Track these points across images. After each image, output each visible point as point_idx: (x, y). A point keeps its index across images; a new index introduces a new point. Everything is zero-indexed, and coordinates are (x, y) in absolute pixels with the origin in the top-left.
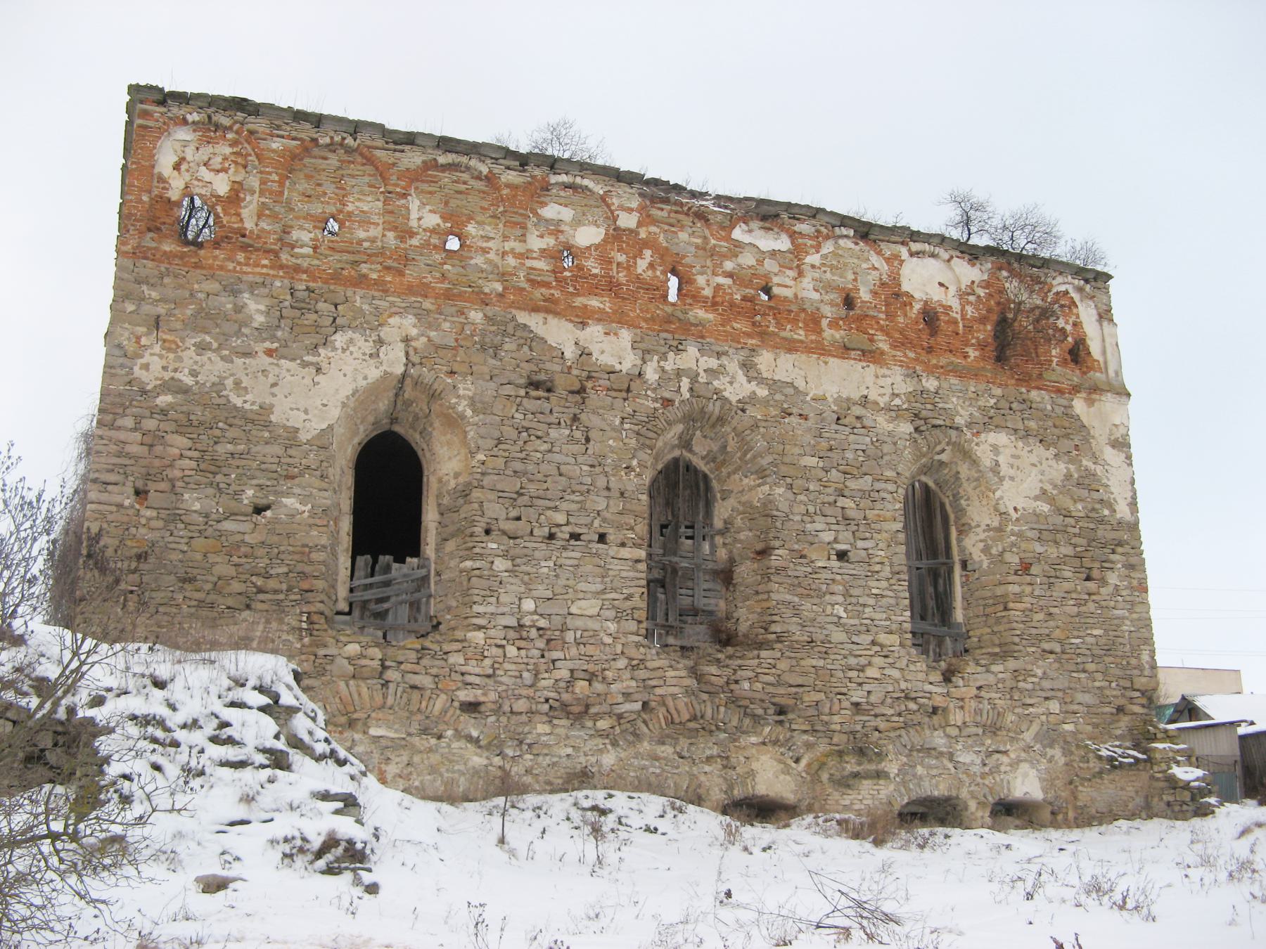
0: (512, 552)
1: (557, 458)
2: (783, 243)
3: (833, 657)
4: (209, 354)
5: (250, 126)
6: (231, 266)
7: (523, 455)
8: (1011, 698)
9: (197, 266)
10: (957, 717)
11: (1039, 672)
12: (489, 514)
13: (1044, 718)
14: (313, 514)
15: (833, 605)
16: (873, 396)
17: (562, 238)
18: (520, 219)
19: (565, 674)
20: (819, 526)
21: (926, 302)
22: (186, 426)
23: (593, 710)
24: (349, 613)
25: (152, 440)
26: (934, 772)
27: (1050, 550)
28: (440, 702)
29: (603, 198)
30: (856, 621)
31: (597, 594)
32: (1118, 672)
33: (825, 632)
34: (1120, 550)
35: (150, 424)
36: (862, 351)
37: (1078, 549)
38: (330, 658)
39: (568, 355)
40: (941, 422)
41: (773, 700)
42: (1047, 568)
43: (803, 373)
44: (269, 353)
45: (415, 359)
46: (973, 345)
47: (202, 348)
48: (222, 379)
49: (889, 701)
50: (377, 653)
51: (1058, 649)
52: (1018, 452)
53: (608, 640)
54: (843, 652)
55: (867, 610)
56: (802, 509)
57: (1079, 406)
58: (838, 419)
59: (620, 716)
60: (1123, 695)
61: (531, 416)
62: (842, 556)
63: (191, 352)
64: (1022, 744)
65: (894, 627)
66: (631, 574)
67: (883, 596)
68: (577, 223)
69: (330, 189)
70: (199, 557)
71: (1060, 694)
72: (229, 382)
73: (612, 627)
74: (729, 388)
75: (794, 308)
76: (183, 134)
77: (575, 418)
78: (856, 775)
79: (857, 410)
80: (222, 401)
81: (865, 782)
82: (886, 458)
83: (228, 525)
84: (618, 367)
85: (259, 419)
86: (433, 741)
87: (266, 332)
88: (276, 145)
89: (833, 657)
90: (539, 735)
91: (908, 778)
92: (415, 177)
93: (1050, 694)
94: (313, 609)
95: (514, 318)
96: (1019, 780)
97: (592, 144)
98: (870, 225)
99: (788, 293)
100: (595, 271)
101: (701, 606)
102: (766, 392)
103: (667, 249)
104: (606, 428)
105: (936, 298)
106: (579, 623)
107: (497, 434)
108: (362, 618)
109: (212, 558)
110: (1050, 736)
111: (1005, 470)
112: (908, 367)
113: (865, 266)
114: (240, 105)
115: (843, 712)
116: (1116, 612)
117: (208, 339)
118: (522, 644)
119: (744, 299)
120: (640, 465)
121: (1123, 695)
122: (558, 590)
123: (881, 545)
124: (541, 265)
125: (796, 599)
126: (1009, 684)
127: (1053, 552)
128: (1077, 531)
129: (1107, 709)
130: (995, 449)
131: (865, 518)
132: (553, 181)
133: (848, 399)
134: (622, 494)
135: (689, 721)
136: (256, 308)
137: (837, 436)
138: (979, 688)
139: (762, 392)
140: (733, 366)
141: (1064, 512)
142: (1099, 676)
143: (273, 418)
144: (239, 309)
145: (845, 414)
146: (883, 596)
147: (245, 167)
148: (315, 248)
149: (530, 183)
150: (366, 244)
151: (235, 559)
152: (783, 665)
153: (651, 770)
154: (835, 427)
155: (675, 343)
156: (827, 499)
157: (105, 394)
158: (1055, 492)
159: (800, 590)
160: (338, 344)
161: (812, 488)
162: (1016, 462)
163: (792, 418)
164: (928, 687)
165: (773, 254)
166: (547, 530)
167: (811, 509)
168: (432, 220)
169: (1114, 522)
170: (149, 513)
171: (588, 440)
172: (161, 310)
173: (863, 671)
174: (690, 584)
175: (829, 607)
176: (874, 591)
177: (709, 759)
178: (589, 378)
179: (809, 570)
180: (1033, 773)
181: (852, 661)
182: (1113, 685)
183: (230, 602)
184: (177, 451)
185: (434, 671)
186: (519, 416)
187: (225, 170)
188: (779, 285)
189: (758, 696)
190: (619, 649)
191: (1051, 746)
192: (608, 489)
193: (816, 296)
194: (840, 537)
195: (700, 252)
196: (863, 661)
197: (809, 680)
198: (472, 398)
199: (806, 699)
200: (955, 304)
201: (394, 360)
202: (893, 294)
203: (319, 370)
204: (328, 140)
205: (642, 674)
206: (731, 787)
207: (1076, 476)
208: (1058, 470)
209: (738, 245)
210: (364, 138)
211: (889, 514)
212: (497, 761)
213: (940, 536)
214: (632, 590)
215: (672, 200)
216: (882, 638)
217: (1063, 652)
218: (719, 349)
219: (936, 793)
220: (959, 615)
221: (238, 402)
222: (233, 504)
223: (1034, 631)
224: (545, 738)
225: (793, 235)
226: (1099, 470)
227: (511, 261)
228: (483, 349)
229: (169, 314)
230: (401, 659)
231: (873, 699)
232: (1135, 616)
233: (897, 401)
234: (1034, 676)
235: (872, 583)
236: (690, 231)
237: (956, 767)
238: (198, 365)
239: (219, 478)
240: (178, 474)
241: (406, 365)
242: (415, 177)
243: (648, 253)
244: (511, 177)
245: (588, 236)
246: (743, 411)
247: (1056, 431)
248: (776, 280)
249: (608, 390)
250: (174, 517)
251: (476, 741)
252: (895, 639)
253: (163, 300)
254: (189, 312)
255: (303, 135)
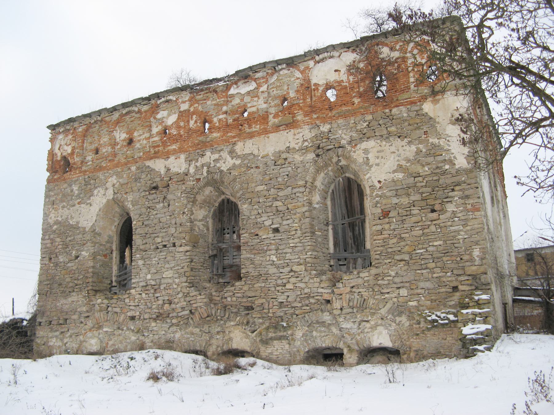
0: (145, 257)
1: (159, 216)
2: (252, 86)
3: (269, 281)
4: (65, 209)
5: (75, 126)
6: (71, 176)
7: (147, 218)
8: (373, 290)
9: (64, 180)
10: (337, 305)
11: (393, 273)
12: (138, 244)
13: (395, 300)
14: (89, 256)
15: (270, 256)
16: (292, 145)
17: (164, 124)
18: (148, 123)
19: (160, 302)
20: (263, 219)
21: (327, 84)
22: (59, 235)
23: (171, 315)
24: (116, 287)
25: (53, 241)
26: (323, 334)
27: (402, 200)
28: (122, 317)
29: (176, 101)
30: (282, 262)
31: (171, 268)
32: (453, 266)
33: (266, 269)
34: (457, 188)
35: (52, 236)
36: (285, 125)
37: (424, 195)
38: (94, 305)
39: (162, 172)
40: (332, 147)
41: (242, 304)
42: (400, 211)
43: (257, 146)
44: (79, 203)
45: (116, 192)
46: (355, 97)
47: (63, 207)
48: (68, 216)
49: (298, 299)
50: (106, 301)
51: (407, 257)
52: (383, 148)
53: (175, 286)
54: (274, 278)
55: (287, 255)
56: (256, 212)
57: (428, 107)
58: (276, 162)
59: (181, 316)
60: (457, 280)
61: (150, 202)
62: (276, 230)
63: (61, 210)
64: (379, 316)
65: (302, 261)
66: (185, 257)
67: (296, 247)
68: (169, 115)
69: (96, 138)
70: (62, 276)
71: (408, 285)
72: (69, 217)
73: (177, 281)
74: (224, 165)
75: (256, 115)
76: (61, 137)
77: (165, 198)
78: (272, 339)
79: (284, 156)
80: (68, 223)
81: (275, 342)
82: (299, 175)
83: (69, 265)
84: (180, 171)
85: (76, 227)
86: (120, 331)
87: (78, 196)
88: (80, 130)
89: (269, 281)
90: (153, 327)
91: (308, 338)
92: (118, 122)
93: (399, 286)
94: (89, 289)
95: (145, 165)
96: (375, 337)
97: (192, 76)
98: (291, 59)
99: (254, 109)
100: (175, 133)
101: (232, 263)
102: (240, 161)
103: (202, 111)
104: (176, 198)
105: (332, 80)
106: (166, 281)
107: (139, 212)
108: (120, 287)
109: (66, 276)
110: (399, 310)
111: (372, 161)
112: (312, 124)
113: (293, 79)
114: (71, 120)
115: (274, 307)
116: (453, 228)
117: (65, 204)
118: (147, 292)
119: (234, 120)
120: (188, 211)
121: (457, 280)
122: (158, 269)
123: (296, 221)
124: (156, 139)
125: (252, 256)
126: (371, 283)
127: (405, 201)
128: (424, 184)
129: (443, 290)
130: (366, 151)
131: (288, 209)
132: (158, 102)
133: (279, 152)
134: (180, 225)
135: (208, 316)
136: (75, 188)
137: (273, 172)
138: (352, 287)
139: (238, 162)
140: (225, 154)
141: (414, 175)
142: (438, 270)
143: (80, 225)
144: (72, 191)
145: (280, 160)
146: (296, 247)
147: (75, 140)
148: (92, 161)
149: (152, 108)
150: (105, 154)
151: (71, 276)
152: (246, 288)
153: (191, 339)
154: (273, 167)
155: (201, 153)
156: (268, 204)
157: (43, 229)
158: (408, 165)
159: (254, 251)
160: (95, 194)
161: (261, 201)
162: (381, 154)
163: (252, 170)
164: (320, 290)
165: (248, 93)
166: (155, 246)
167: (260, 211)
168: (124, 136)
169: (453, 171)
170: (52, 265)
171: (169, 205)
172: (54, 199)
173: (285, 286)
174: (228, 254)
175: (268, 257)
176: (291, 245)
177: (218, 333)
178: (171, 179)
179: (259, 241)
180: (385, 332)
181: (279, 282)
182: (449, 274)
183: (70, 290)
184: (57, 243)
185: (120, 306)
186: (147, 203)
187: (70, 144)
188: (251, 107)
189: (234, 303)
190: (179, 289)
191: (400, 314)
192: (176, 224)
193: (265, 106)
194: (274, 222)
195: (216, 107)
196: (284, 281)
197: (258, 294)
198: (132, 201)
199: (256, 302)
200: (344, 77)
201: (110, 194)
202: (307, 87)
203: (91, 205)
204: (93, 121)
205: (188, 299)
206: (223, 346)
207: (424, 150)
208: (410, 151)
209: (232, 96)
210: (103, 115)
211: (300, 204)
212: (141, 338)
213: (356, 203)
214: (184, 265)
215: (204, 89)
216: (295, 268)
217: (411, 259)
218: (219, 149)
219: (324, 345)
220: (368, 246)
221: (71, 222)
222: (70, 257)
223: (390, 250)
224: (155, 328)
225: (255, 80)
226: (442, 142)
227: (145, 142)
228: (136, 181)
229: (56, 199)
230: (112, 303)
231: (289, 299)
232: (468, 228)
233: (306, 144)
234: (390, 276)
235: (291, 241)
236: (211, 99)
237: (346, 330)
238: (61, 214)
239: (67, 249)
240: (57, 250)
241: (114, 195)
242: (118, 122)
243: (194, 116)
244: (145, 108)
245: (172, 120)
246: (230, 174)
247: (410, 127)
248: (249, 105)
249: (178, 182)
250: (56, 265)
251: (133, 331)
252: (302, 267)
253: (55, 195)
254: (60, 196)
255: (87, 123)
